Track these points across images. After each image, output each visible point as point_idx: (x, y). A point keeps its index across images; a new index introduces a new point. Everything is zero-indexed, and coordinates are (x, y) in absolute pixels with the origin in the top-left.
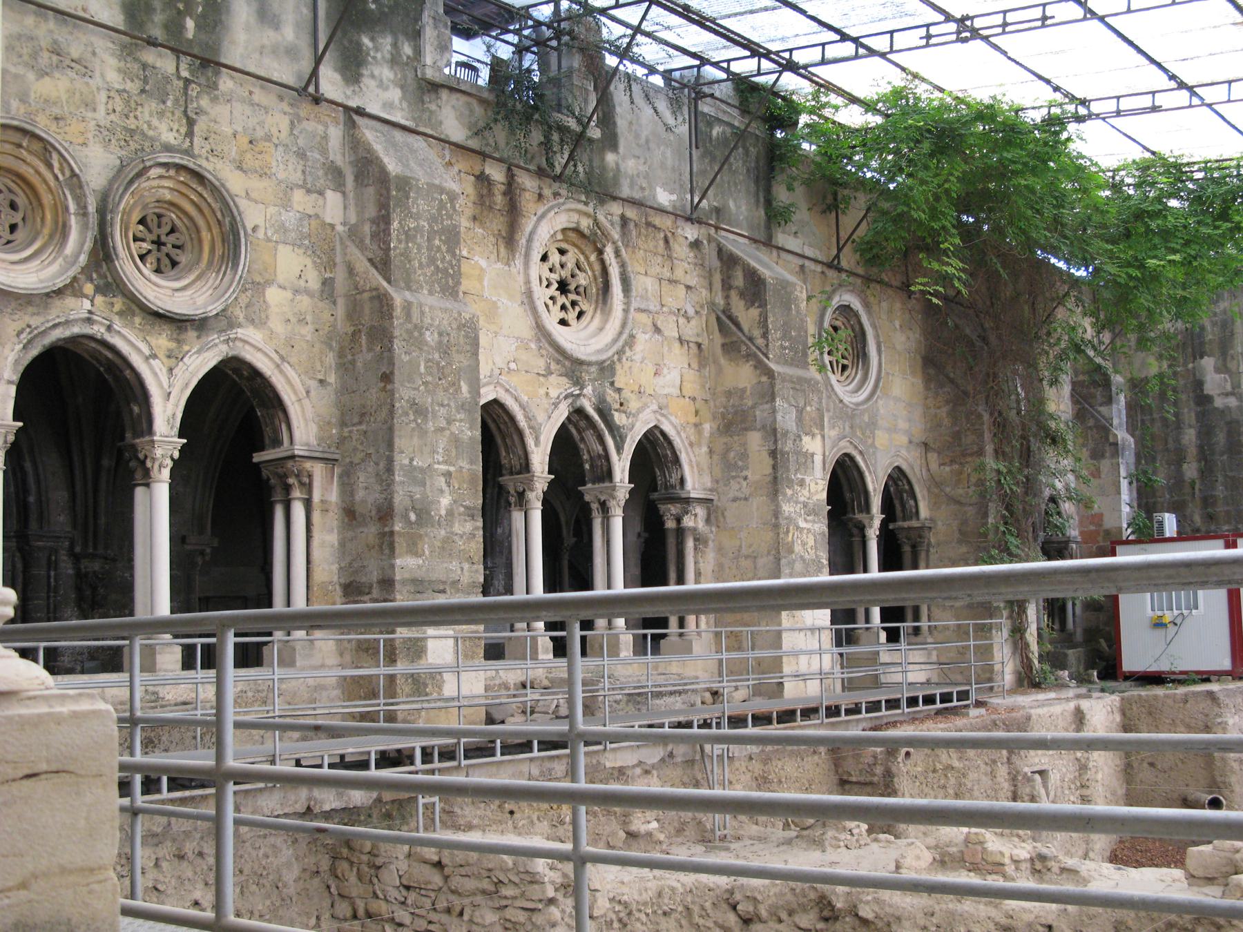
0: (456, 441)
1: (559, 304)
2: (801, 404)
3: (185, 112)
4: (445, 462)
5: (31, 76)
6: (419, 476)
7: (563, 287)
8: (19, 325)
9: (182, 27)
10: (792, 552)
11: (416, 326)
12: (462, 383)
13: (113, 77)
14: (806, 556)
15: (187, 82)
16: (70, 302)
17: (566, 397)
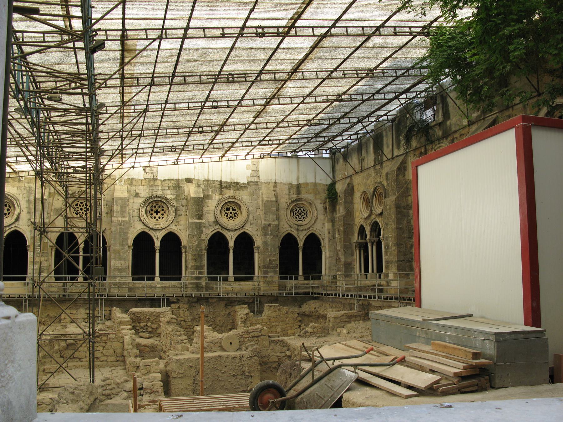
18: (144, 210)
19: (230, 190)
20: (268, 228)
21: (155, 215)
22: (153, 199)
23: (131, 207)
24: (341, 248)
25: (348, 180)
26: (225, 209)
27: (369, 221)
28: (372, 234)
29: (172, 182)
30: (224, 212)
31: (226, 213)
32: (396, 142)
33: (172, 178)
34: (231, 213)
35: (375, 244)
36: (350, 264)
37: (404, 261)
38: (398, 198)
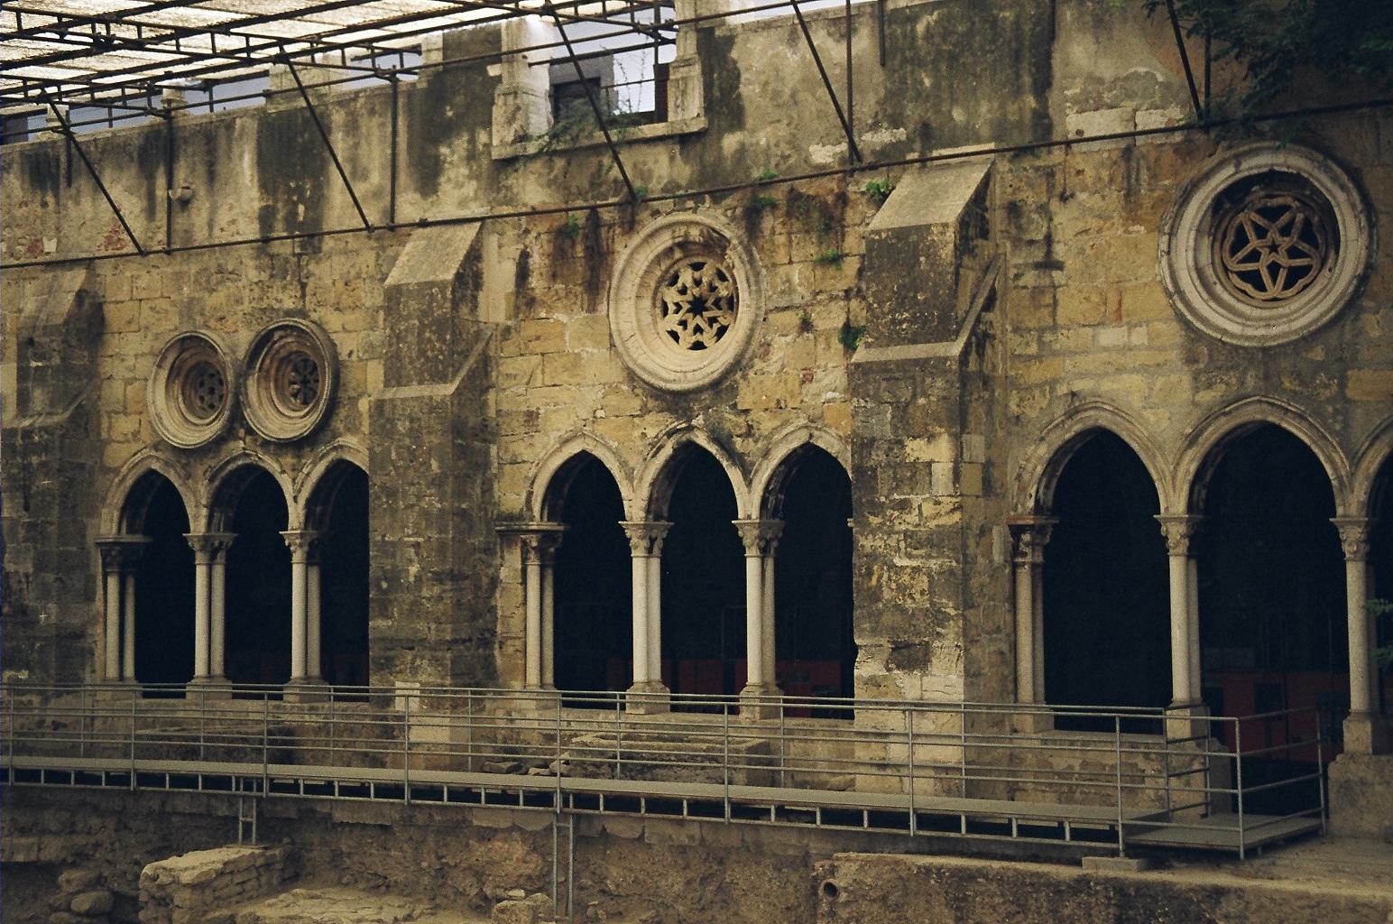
0: (426, 514)
1: (691, 327)
2: (905, 395)
3: (299, 281)
4: (413, 535)
5: (206, 295)
6: (390, 549)
7: (697, 306)
8: (205, 467)
9: (297, 214)
10: (878, 600)
11: (388, 420)
12: (433, 461)
13: (253, 275)
14: (909, 604)
15: (299, 255)
16: (232, 445)
17: (670, 434)
24: (40, 566)
25: (76, 278)
27: (213, 463)
28: (217, 515)
32: (410, 165)
35: (221, 557)
36: (79, 635)
37: (470, 640)
38: (458, 392)
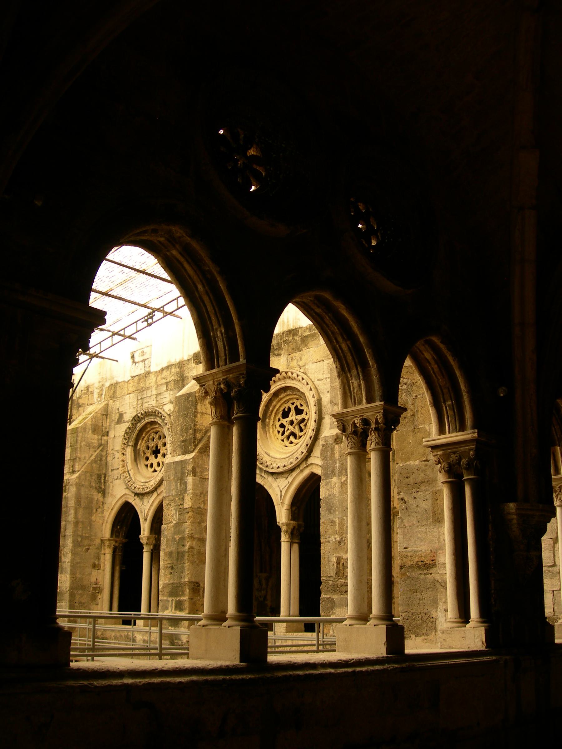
18: (129, 451)
19: (279, 355)
20: (333, 449)
21: (152, 459)
22: (143, 423)
23: (111, 448)
26: (280, 416)
29: (173, 370)
30: (278, 424)
31: (282, 426)
33: (173, 361)
34: (292, 423)
